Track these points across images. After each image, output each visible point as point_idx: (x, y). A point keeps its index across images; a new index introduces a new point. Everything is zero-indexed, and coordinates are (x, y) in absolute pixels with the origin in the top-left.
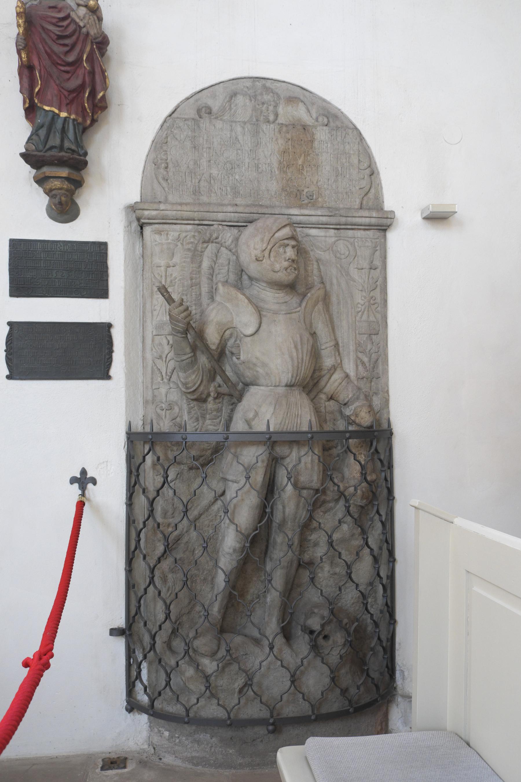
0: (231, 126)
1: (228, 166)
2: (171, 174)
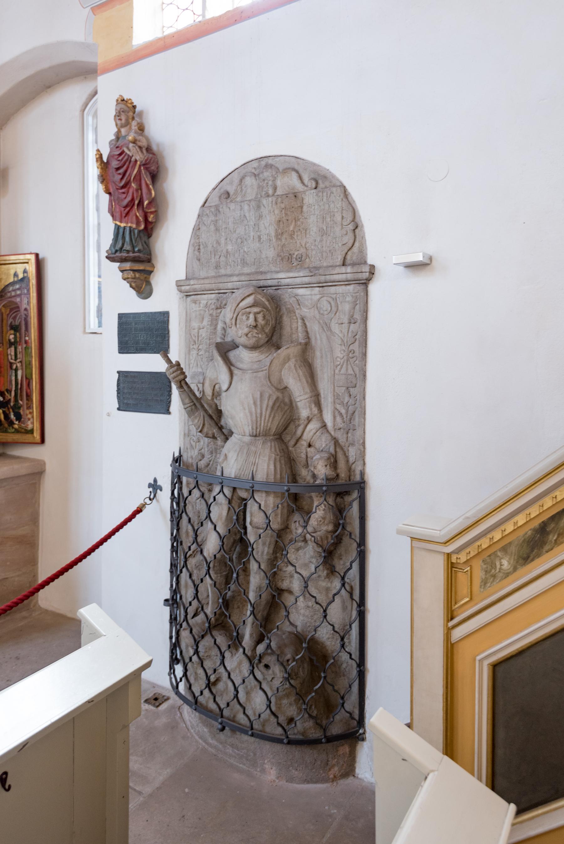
0: (241, 206)
1: (239, 241)
2: (201, 254)
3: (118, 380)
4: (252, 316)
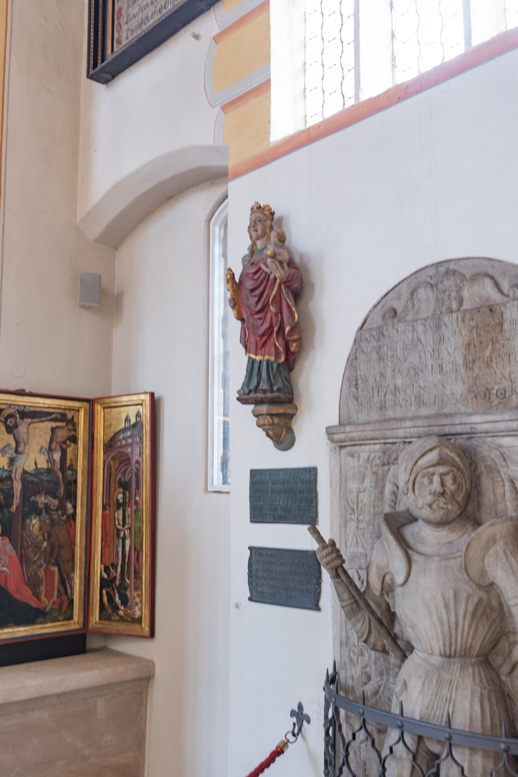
1: (412, 372)
2: (360, 391)
3: (250, 559)
4: (436, 479)
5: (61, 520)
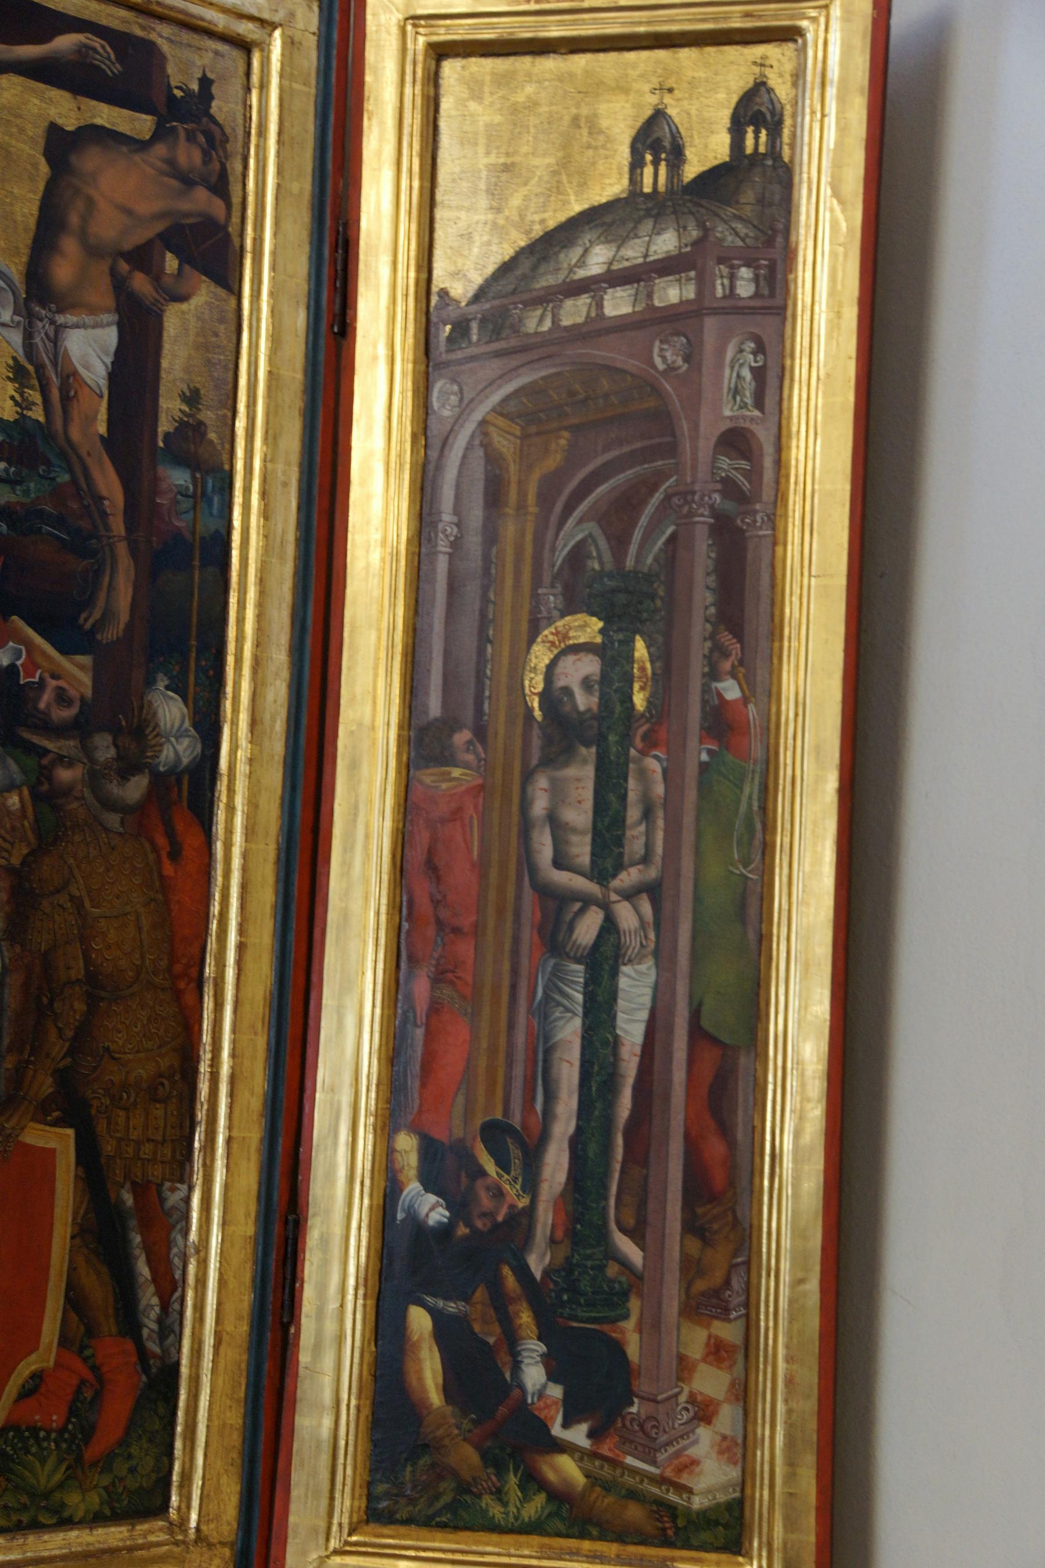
5: (110, 805)
